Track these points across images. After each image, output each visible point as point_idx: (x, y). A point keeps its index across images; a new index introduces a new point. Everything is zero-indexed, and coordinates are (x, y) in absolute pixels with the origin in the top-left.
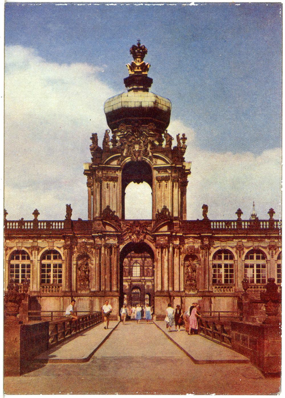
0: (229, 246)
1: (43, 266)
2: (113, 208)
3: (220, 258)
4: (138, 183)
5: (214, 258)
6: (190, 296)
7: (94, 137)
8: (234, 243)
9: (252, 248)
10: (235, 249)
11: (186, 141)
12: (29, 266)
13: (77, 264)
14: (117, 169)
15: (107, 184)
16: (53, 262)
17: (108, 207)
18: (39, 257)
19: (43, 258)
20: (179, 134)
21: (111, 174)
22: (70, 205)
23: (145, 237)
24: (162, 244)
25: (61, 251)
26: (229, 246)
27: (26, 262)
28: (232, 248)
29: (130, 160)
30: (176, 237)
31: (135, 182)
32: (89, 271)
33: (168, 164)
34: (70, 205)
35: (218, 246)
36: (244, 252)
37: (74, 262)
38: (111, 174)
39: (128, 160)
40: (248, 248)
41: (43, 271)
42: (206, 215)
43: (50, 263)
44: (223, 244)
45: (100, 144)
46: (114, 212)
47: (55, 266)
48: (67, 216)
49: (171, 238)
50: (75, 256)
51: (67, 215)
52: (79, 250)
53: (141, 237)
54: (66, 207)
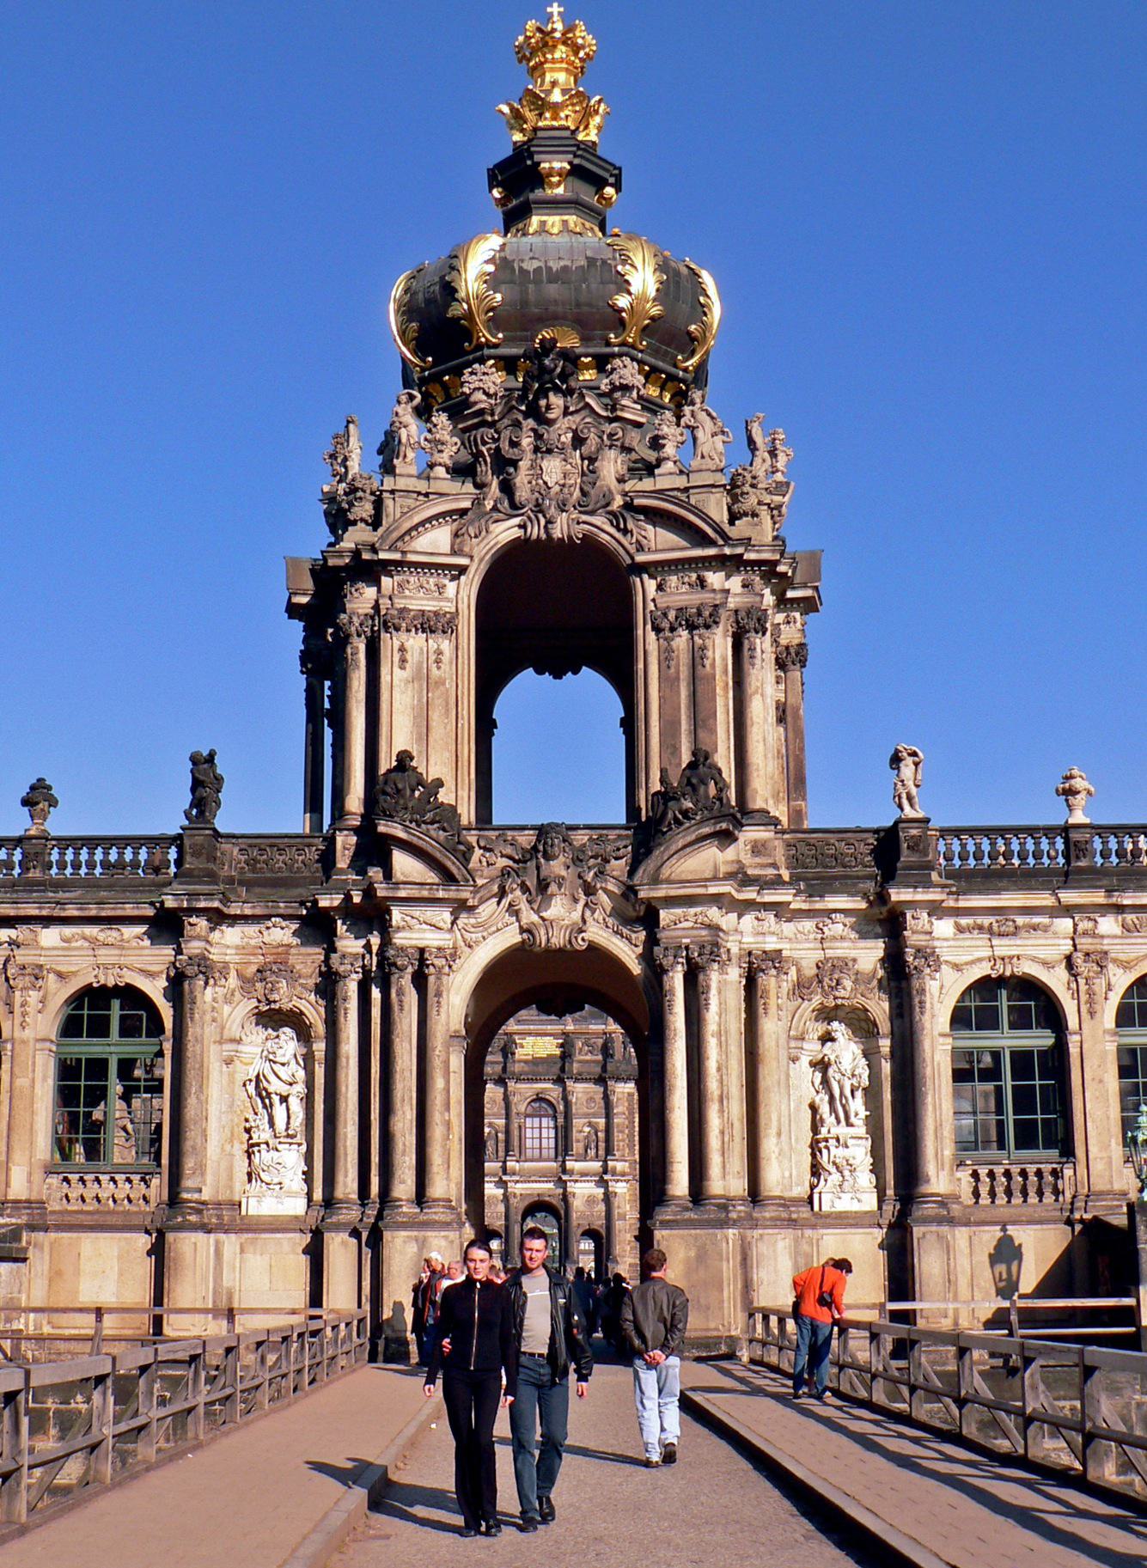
0: (1034, 959)
2: (435, 766)
4: (558, 675)
17: (404, 759)
19: (71, 1028)
21: (417, 596)
22: (212, 755)
24: (687, 948)
26: (1034, 959)
28: (1048, 965)
29: (518, 533)
31: (540, 672)
33: (712, 543)
34: (212, 755)
35: (980, 960)
36: (1109, 988)
38: (417, 596)
39: (505, 532)
40: (1126, 966)
41: (66, 1096)
43: (104, 1056)
44: (1004, 947)
46: (439, 783)
48: (194, 812)
51: (191, 806)
54: (190, 766)
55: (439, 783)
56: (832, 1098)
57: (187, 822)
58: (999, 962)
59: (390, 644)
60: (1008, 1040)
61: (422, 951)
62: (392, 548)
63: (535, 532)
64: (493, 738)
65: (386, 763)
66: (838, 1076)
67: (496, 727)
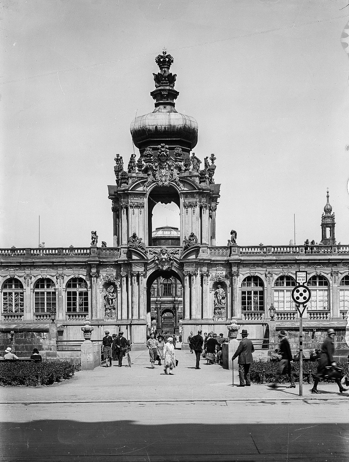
1: (69, 293)
5: (243, 284)
7: (119, 160)
11: (215, 161)
12: (54, 293)
14: (143, 194)
18: (64, 285)
20: (207, 158)
22: (95, 232)
27: (51, 290)
33: (196, 189)
34: (95, 232)
41: (69, 299)
42: (235, 242)
45: (126, 169)
46: (141, 239)
47: (81, 294)
55: (141, 239)
56: (218, 300)
57: (91, 246)
58: (251, 273)
59: (130, 210)
60: (253, 288)
61: (138, 272)
62: (131, 190)
63: (160, 184)
64: (152, 218)
65: (131, 235)
66: (219, 295)
67: (153, 215)
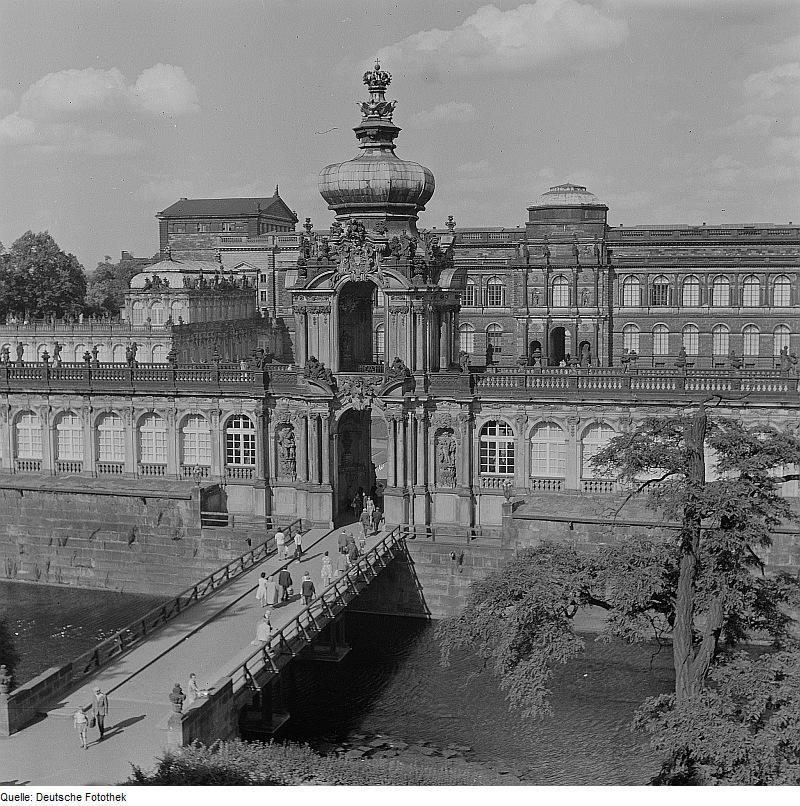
3: (493, 432)
6: (443, 492)
8: (514, 410)
9: (540, 420)
10: (514, 421)
13: (277, 437)
15: (314, 319)
16: (241, 431)
18: (222, 424)
21: (321, 303)
23: (371, 401)
25: (253, 418)
30: (419, 403)
32: (294, 447)
37: (272, 434)
38: (321, 303)
49: (408, 405)
50: (272, 426)
52: (278, 416)
53: (366, 401)
